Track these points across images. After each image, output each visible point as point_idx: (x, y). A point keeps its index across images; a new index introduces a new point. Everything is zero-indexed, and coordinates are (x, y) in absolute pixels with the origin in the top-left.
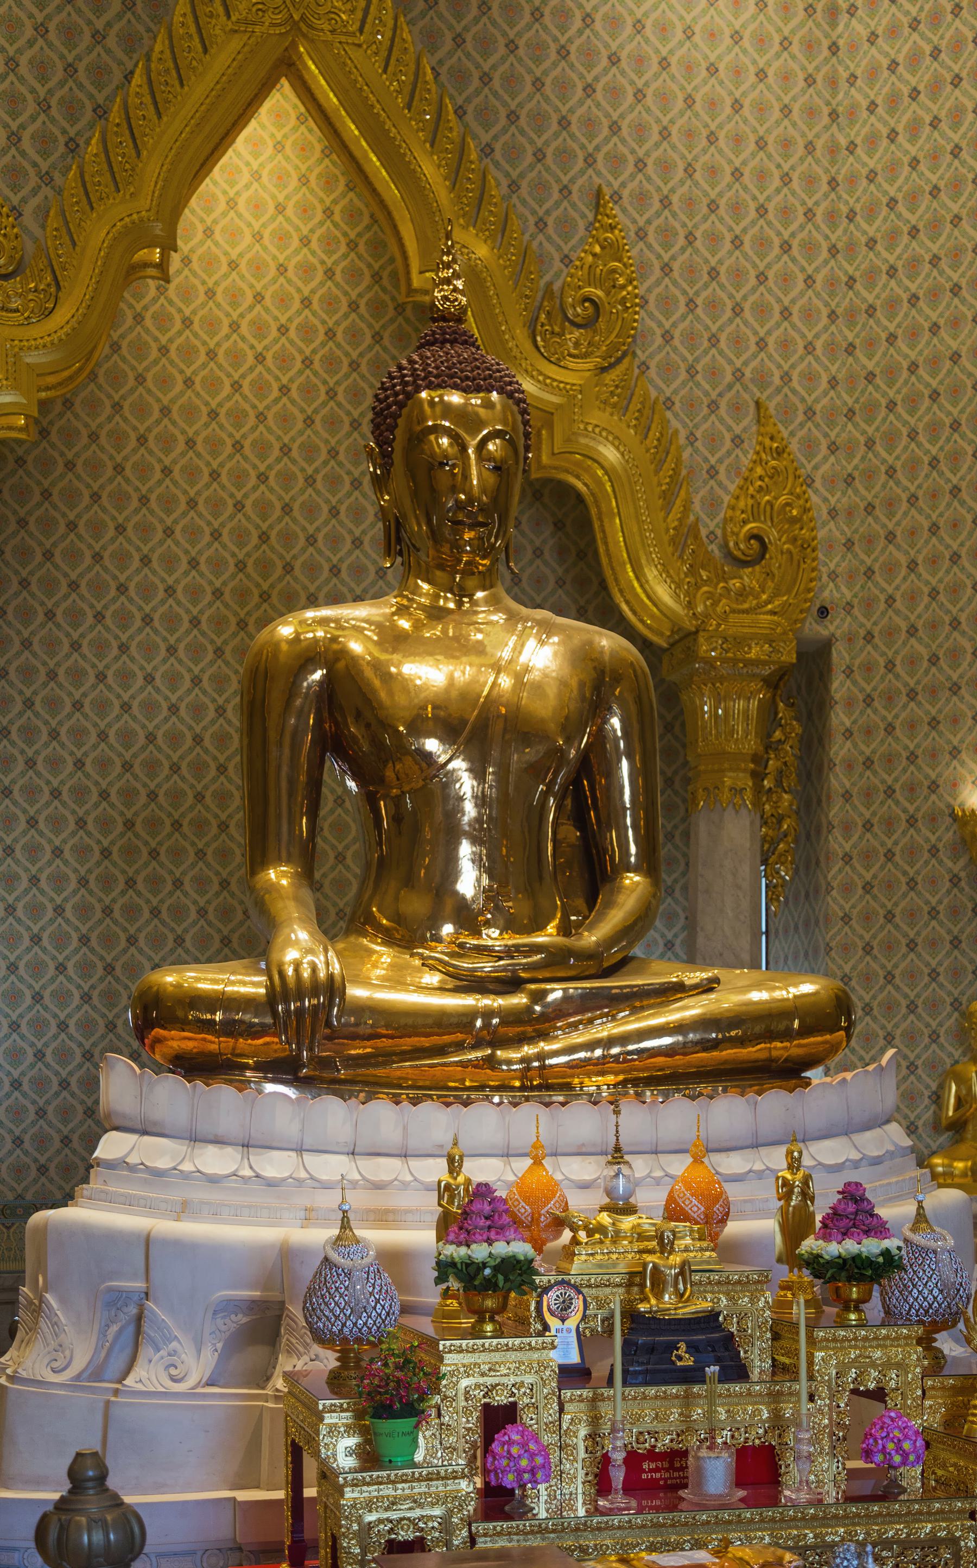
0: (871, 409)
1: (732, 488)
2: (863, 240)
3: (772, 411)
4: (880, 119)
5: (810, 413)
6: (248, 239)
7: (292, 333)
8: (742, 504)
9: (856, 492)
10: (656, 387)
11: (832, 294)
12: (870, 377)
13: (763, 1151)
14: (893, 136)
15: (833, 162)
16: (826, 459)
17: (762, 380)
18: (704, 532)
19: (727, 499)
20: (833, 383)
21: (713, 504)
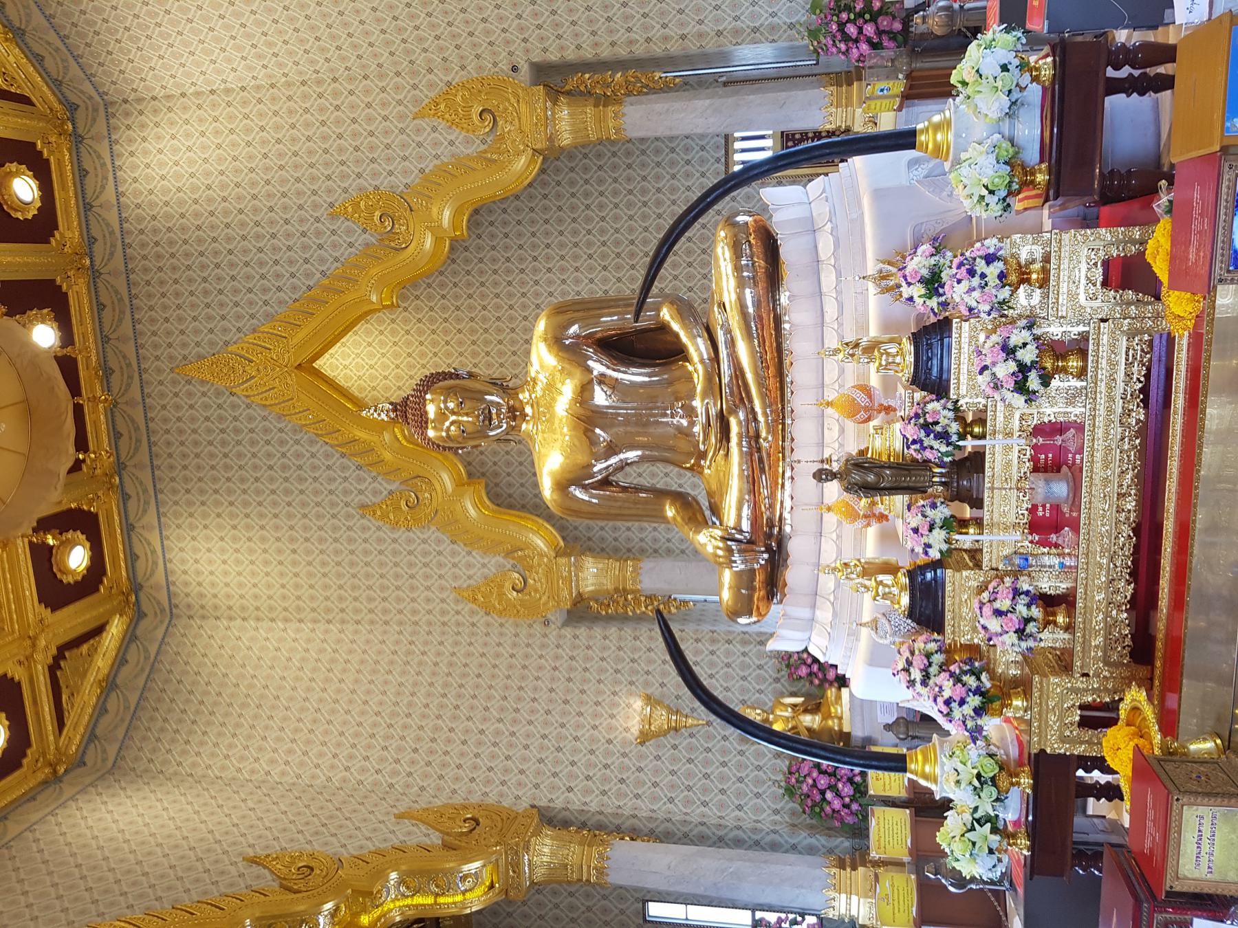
0: (408, 52)
1: (458, 131)
2: (327, 64)
3: (416, 110)
4: (269, 62)
5: (415, 87)
6: (385, 359)
7: (422, 339)
8: (465, 126)
9: (450, 55)
10: (415, 178)
11: (356, 79)
12: (392, 54)
13: (824, 289)
14: (275, 55)
15: (294, 84)
16: (436, 75)
17: (401, 117)
18: (483, 147)
19: (464, 133)
20: (398, 74)
21: (467, 142)
